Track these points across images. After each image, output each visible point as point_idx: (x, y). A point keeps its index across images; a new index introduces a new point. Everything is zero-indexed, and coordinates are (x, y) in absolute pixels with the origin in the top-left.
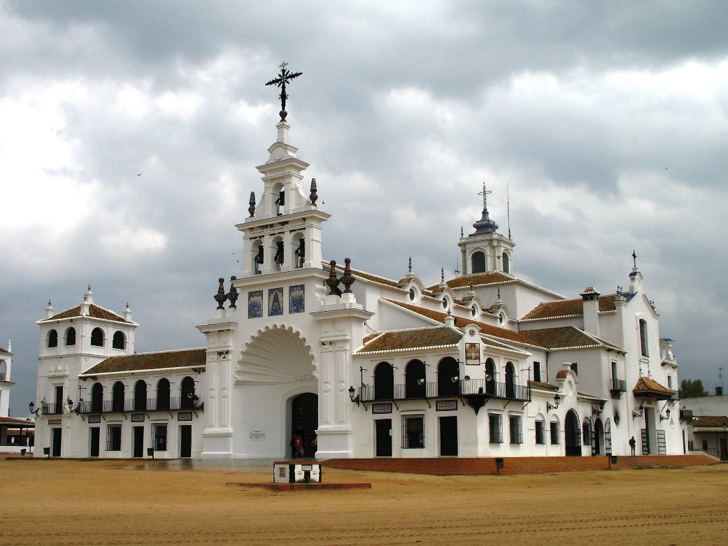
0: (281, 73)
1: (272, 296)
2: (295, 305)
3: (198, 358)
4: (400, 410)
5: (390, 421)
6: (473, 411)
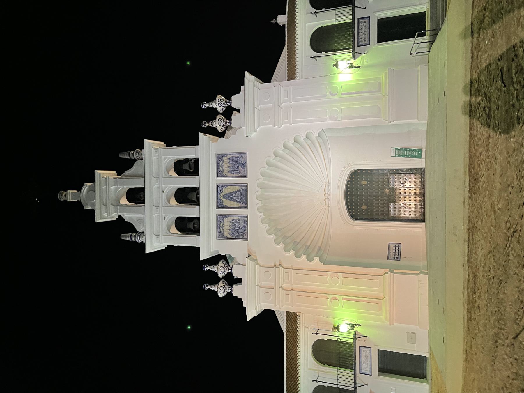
1: (227, 203)
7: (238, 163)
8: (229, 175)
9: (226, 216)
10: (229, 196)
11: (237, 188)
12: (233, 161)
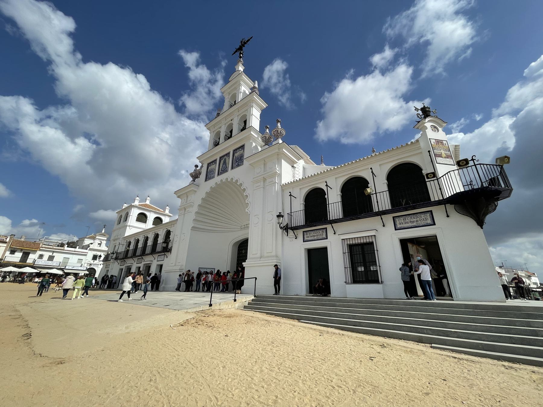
1: (222, 162)
2: (237, 162)
4: (337, 234)
5: (325, 249)
6: (469, 223)
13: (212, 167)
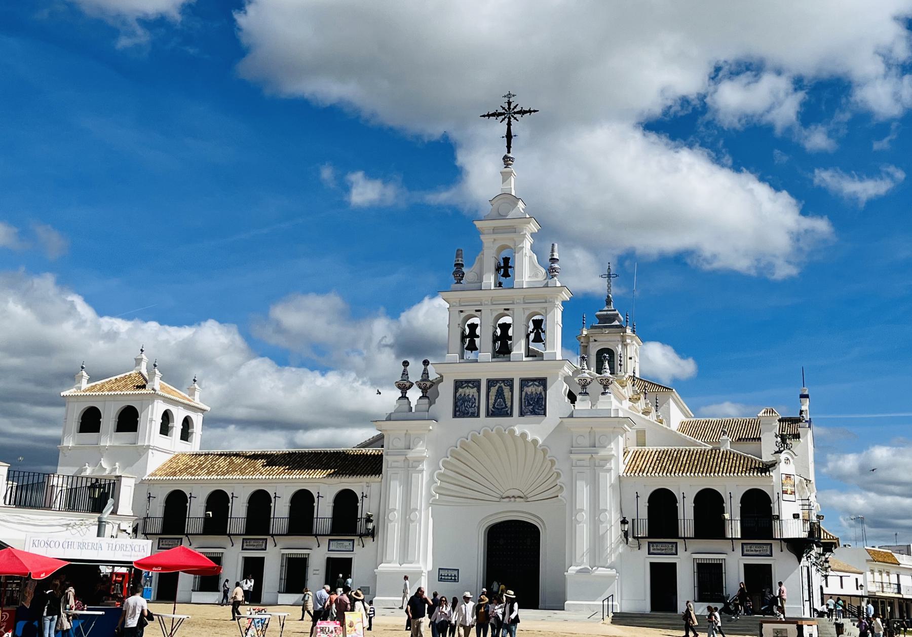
0: (506, 107)
1: (494, 390)
2: (529, 404)
3: (368, 464)
5: (674, 565)
7: (535, 405)
8: (524, 394)
9: (479, 391)
10: (500, 393)
11: (509, 404)
12: (539, 398)
13: (471, 392)
